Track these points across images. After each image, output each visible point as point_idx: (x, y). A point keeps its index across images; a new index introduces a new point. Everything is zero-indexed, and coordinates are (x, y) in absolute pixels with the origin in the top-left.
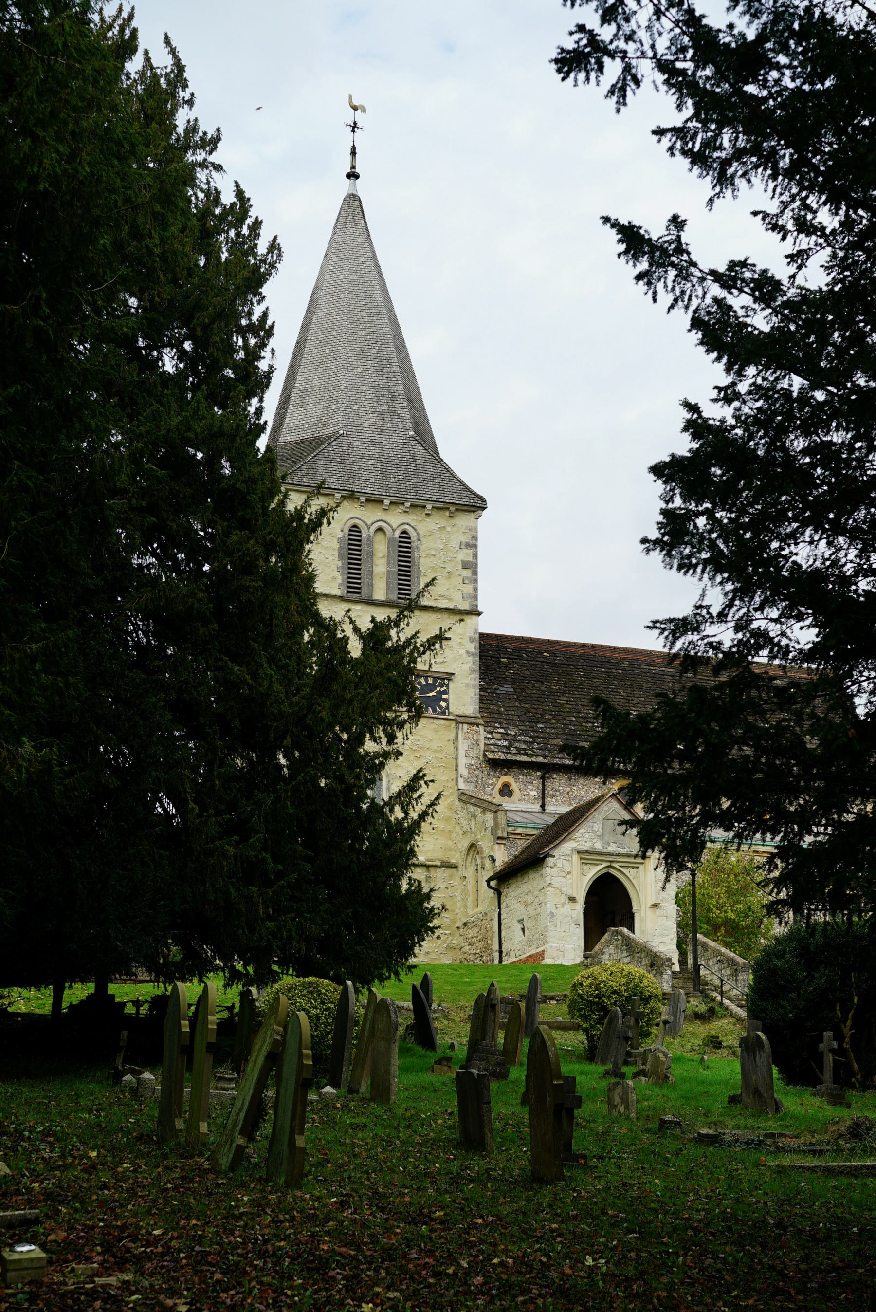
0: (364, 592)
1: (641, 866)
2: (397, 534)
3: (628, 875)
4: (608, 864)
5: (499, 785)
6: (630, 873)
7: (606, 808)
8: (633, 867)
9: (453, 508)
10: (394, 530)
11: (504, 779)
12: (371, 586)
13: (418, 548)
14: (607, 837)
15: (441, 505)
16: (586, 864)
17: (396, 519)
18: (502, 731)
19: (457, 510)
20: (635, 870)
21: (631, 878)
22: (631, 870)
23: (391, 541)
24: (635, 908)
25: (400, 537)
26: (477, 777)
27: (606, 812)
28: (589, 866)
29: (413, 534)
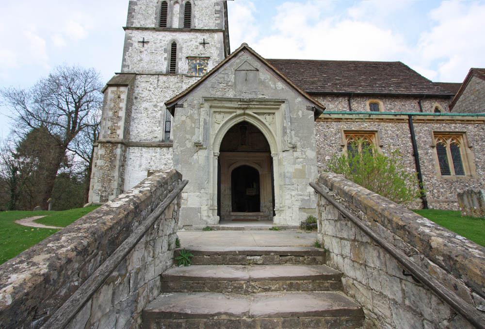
0: (168, 25)
3: (264, 121)
4: (241, 112)
6: (266, 120)
7: (238, 61)
8: (269, 114)
12: (171, 22)
14: (239, 87)
16: (220, 112)
20: (271, 116)
21: (267, 124)
22: (267, 117)
23: (181, 6)
25: (186, 4)
27: (237, 64)
28: (222, 115)
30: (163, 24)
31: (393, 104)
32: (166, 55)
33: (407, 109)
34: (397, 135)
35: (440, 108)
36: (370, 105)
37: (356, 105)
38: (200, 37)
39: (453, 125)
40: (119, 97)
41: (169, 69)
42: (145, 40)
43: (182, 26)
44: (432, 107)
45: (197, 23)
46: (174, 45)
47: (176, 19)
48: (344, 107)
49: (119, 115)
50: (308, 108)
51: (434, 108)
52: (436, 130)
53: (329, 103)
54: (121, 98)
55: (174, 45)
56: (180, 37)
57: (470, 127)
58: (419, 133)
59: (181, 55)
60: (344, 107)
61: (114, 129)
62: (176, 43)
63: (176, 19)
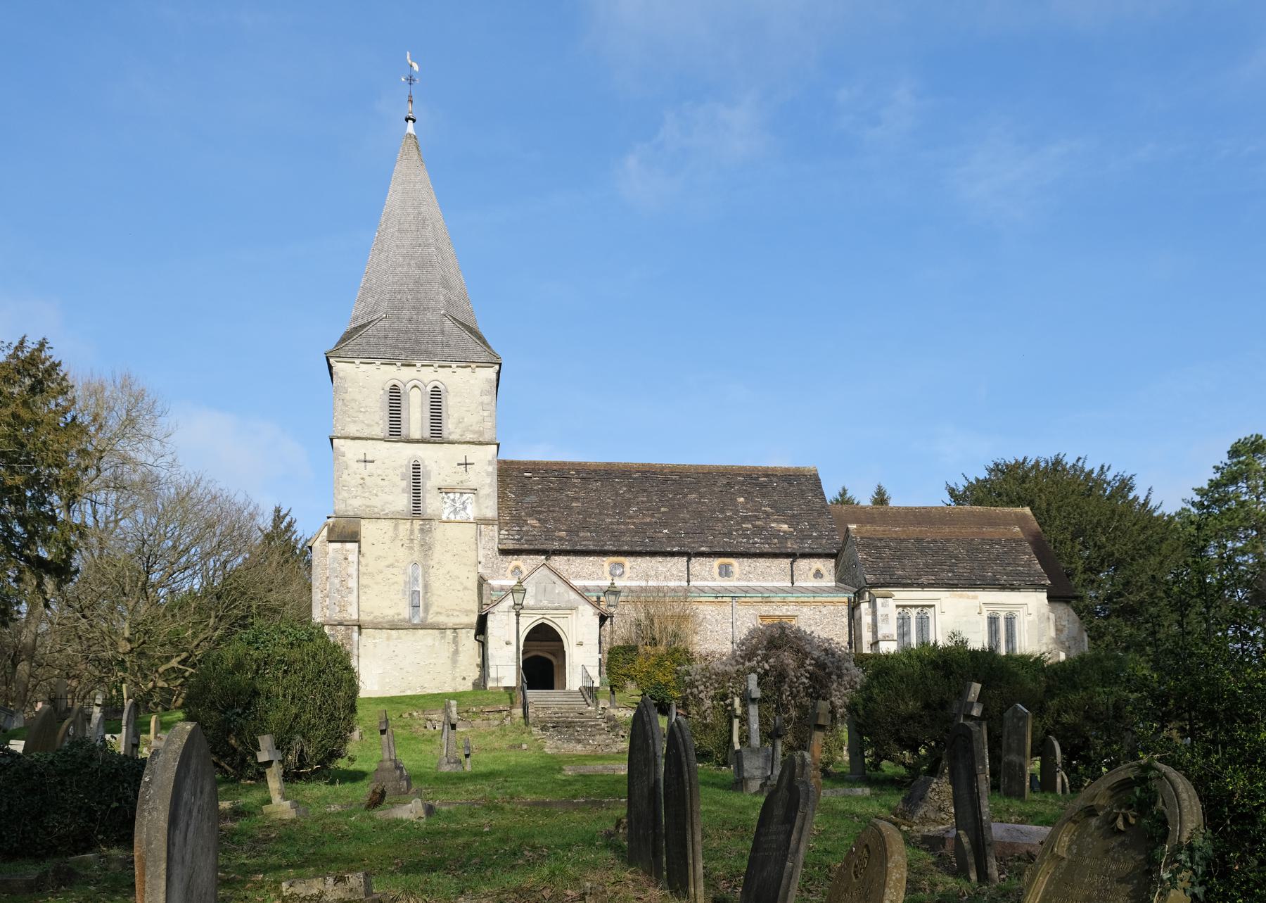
0: (404, 431)
1: (569, 616)
2: (429, 388)
5: (511, 567)
9: (474, 365)
10: (426, 386)
11: (515, 563)
13: (446, 397)
15: (464, 364)
17: (428, 375)
18: (517, 528)
19: (477, 367)
24: (566, 648)
26: (493, 563)
29: (441, 387)
30: (395, 433)
31: (752, 565)
32: (404, 483)
33: (773, 572)
34: (717, 620)
35: (823, 571)
36: (720, 567)
37: (698, 568)
38: (459, 452)
39: (786, 607)
40: (346, 559)
41: (412, 508)
42: (367, 459)
43: (427, 434)
44: (810, 569)
45: (450, 427)
46: (416, 467)
47: (416, 418)
48: (681, 571)
49: (350, 586)
50: (594, 614)
51: (813, 571)
52: (763, 614)
53: (659, 565)
54: (350, 559)
55: (416, 467)
56: (427, 454)
57: (805, 609)
58: (743, 617)
59: (429, 485)
60: (681, 571)
61: (344, 606)
62: (420, 463)
63: (416, 418)
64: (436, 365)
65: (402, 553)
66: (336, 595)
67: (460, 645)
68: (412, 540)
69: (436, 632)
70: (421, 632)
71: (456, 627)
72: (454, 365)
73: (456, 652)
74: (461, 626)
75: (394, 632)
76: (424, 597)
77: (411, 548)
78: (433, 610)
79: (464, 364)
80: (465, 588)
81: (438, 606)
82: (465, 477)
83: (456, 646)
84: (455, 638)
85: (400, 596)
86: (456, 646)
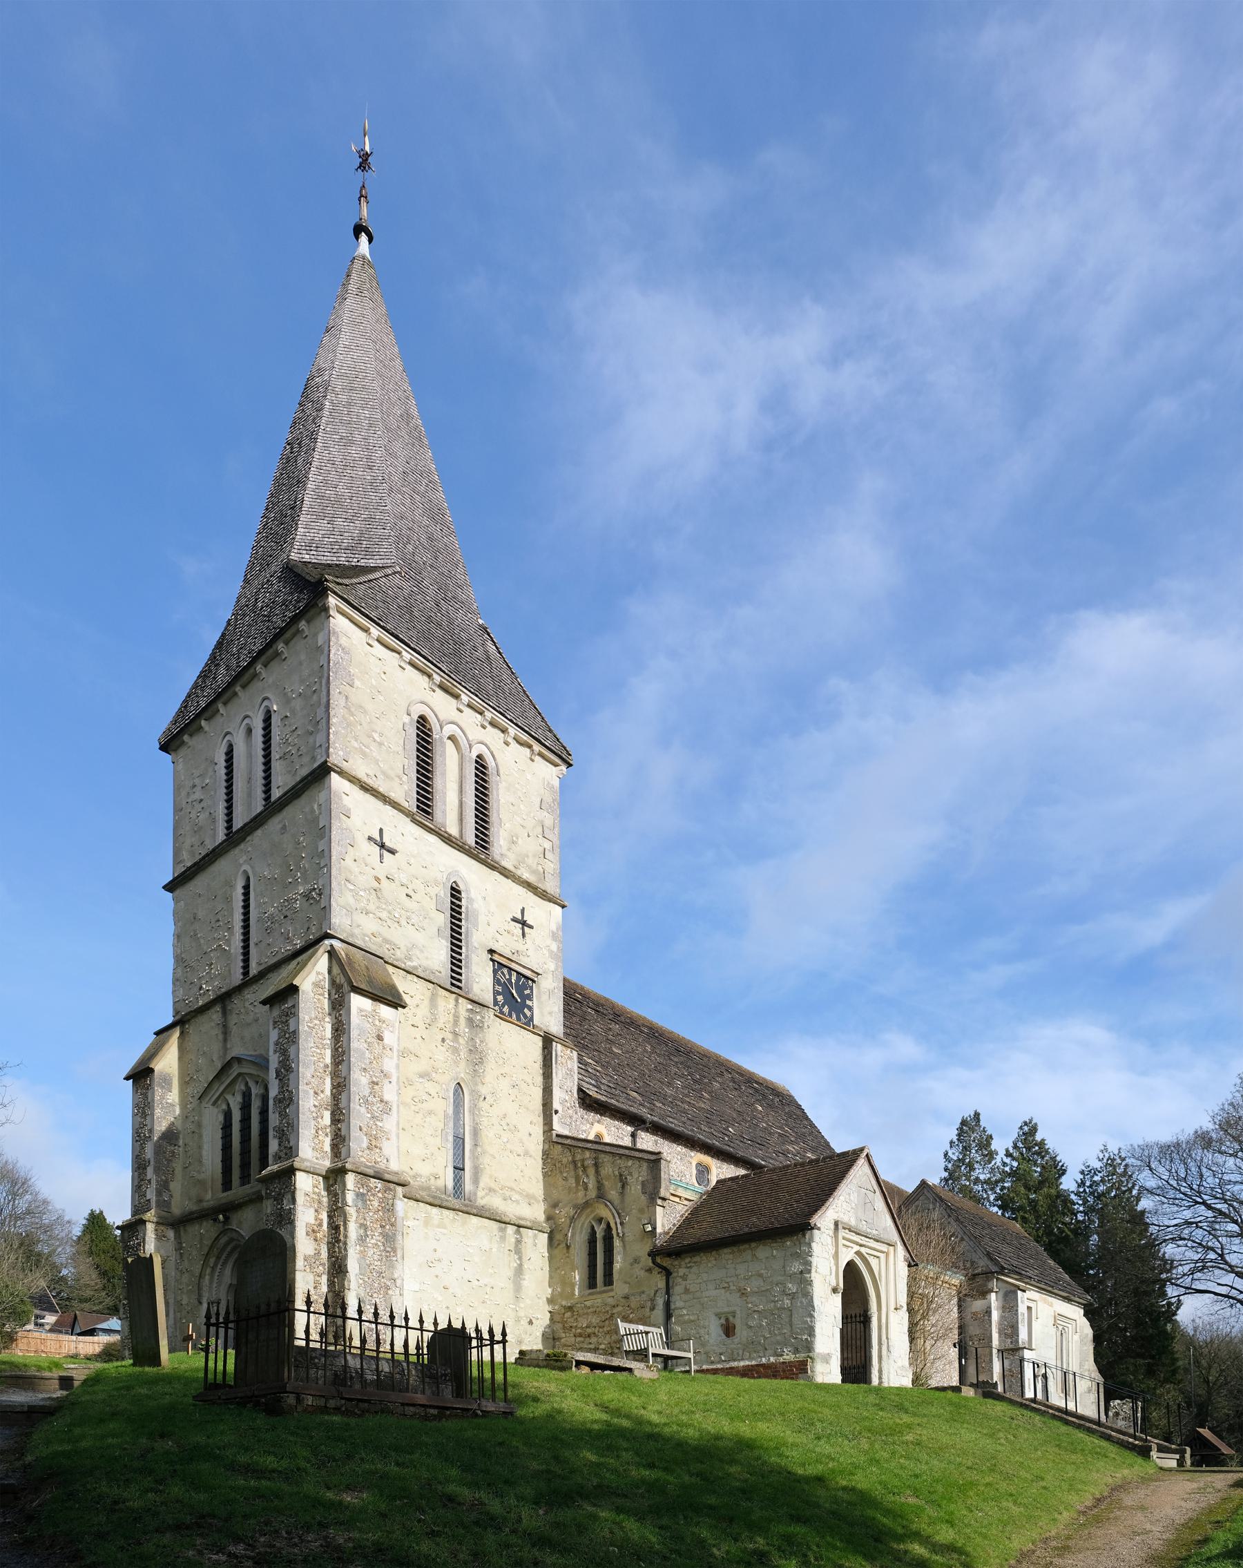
46: (455, 892)
55: (455, 892)
64: (488, 715)
65: (441, 1055)
66: (363, 1110)
67: (525, 1259)
68: (455, 1034)
69: (495, 1225)
70: (474, 1220)
71: (522, 1223)
72: (513, 730)
73: (519, 1270)
74: (529, 1224)
75: (435, 1210)
76: (473, 1152)
77: (456, 1051)
78: (485, 1181)
79: (525, 737)
80: (527, 1153)
81: (491, 1177)
82: (521, 947)
83: (520, 1259)
84: (518, 1242)
85: (438, 1141)
86: (520, 1259)
